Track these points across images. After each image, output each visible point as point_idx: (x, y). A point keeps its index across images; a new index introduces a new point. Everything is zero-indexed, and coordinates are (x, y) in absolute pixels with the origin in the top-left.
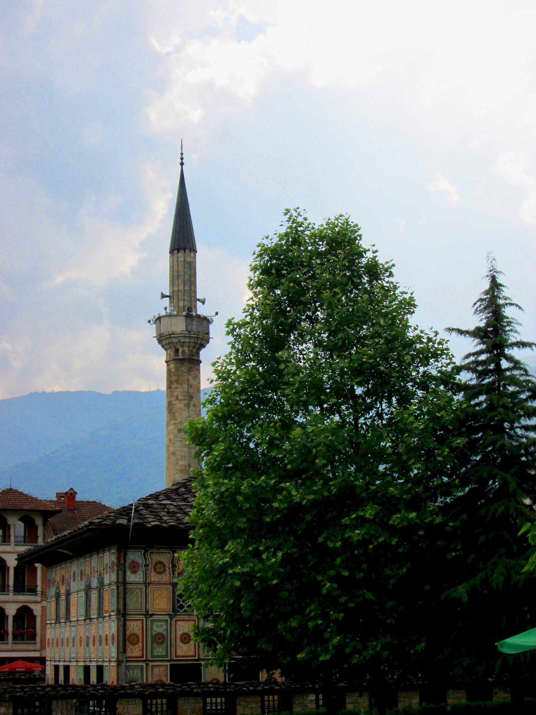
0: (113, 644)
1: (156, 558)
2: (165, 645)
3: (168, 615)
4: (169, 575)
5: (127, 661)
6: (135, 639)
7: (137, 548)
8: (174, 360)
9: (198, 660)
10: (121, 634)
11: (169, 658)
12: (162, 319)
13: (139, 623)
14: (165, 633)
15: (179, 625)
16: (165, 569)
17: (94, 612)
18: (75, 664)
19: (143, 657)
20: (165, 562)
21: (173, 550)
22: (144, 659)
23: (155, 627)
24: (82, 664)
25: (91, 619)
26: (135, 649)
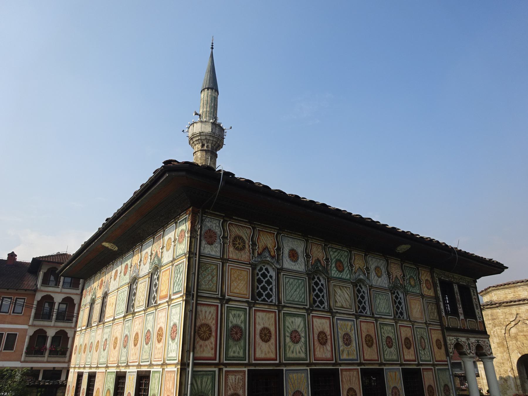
1: (236, 231)
2: (242, 342)
3: (247, 302)
7: (217, 216)
8: (201, 150)
13: (213, 309)
14: (243, 326)
15: (259, 317)
16: (245, 246)
18: (103, 370)
19: (215, 360)
20: (245, 238)
22: (217, 361)
23: (231, 317)
24: (114, 370)
25: (134, 313)
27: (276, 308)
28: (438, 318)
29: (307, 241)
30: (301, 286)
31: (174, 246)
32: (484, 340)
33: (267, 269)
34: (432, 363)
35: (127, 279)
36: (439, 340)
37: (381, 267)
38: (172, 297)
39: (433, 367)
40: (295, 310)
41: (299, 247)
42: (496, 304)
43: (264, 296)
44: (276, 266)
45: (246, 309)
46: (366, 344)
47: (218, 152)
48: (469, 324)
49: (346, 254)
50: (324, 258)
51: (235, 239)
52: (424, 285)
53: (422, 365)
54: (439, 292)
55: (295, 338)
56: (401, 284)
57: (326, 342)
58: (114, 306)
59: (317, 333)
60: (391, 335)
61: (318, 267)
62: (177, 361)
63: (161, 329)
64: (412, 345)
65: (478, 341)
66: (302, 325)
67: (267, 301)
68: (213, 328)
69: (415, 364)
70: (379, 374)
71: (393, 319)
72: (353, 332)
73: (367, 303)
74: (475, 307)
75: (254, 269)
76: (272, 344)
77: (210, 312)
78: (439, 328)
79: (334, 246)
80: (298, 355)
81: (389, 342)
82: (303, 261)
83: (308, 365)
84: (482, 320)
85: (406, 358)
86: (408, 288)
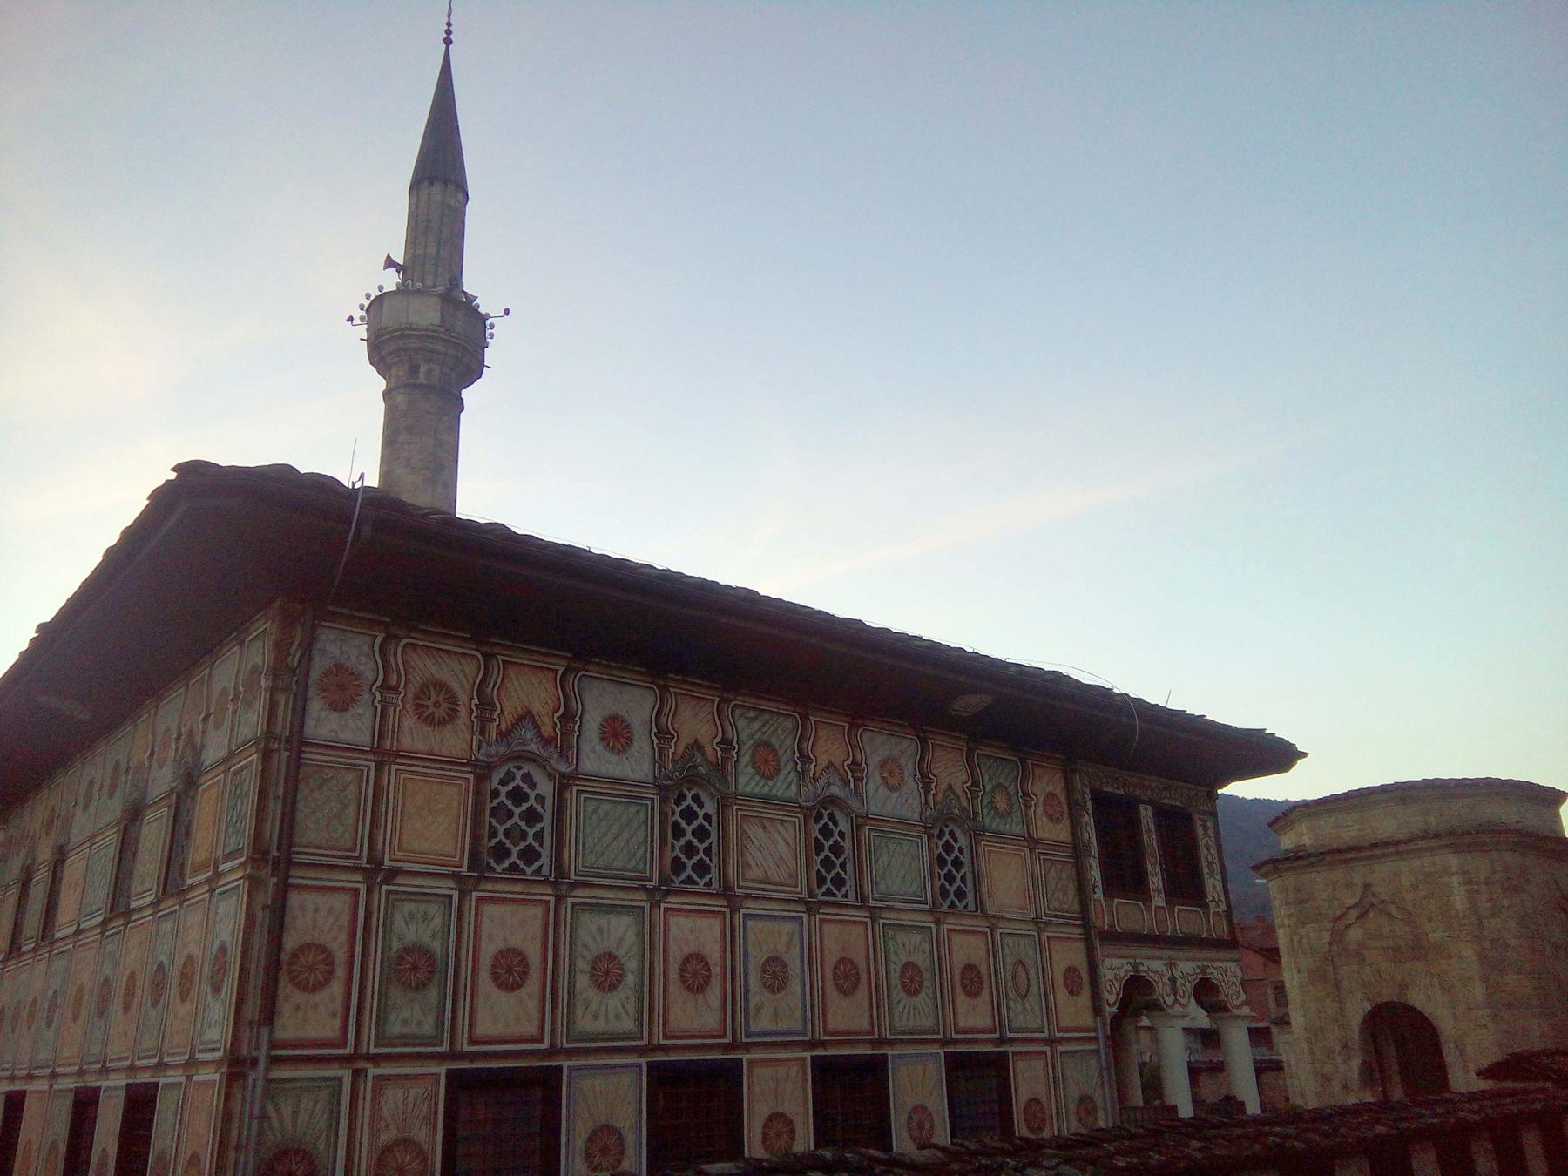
0: (216, 989)
1: (426, 667)
2: (432, 994)
3: (453, 876)
4: (468, 736)
5: (276, 1061)
6: (315, 968)
8: (406, 386)
9: (552, 1052)
10: (260, 941)
11: (445, 1048)
12: (386, 305)
13: (341, 902)
14: (436, 946)
17: (147, 885)
18: (43, 1085)
20: (455, 686)
21: (486, 649)
22: (349, 1050)
25: (128, 913)
26: (316, 1007)
27: (550, 891)
28: (1076, 907)
29: (663, 690)
30: (635, 825)
31: (234, 712)
32: (1222, 964)
33: (527, 778)
34: (1046, 1035)
35: (114, 808)
36: (1075, 970)
37: (903, 761)
38: (222, 868)
39: (1047, 1049)
40: (610, 894)
41: (635, 704)
42: (1310, 856)
43: (514, 858)
44: (557, 766)
45: (450, 897)
46: (836, 985)
47: (465, 393)
48: (1184, 920)
49: (789, 724)
50: (718, 739)
51: (422, 691)
52: (1040, 810)
53: (1012, 1041)
54: (1090, 834)
55: (606, 973)
56: (963, 810)
57: (707, 983)
58: (79, 889)
59: (679, 959)
60: (920, 960)
61: (695, 766)
62: (221, 1054)
63: (190, 958)
64: (986, 986)
65: (1203, 970)
66: (631, 937)
67: (523, 872)
68: (340, 955)
69: (991, 1041)
70: (874, 1069)
71: (930, 911)
72: (797, 951)
73: (849, 866)
74: (1206, 870)
75: (480, 780)
76: (530, 996)
77: (330, 910)
78: (1077, 933)
79: (751, 701)
80: (614, 1026)
81: (912, 981)
82: (647, 749)
83: (642, 1051)
84: (1223, 906)
85: (962, 1023)
86: (987, 820)
